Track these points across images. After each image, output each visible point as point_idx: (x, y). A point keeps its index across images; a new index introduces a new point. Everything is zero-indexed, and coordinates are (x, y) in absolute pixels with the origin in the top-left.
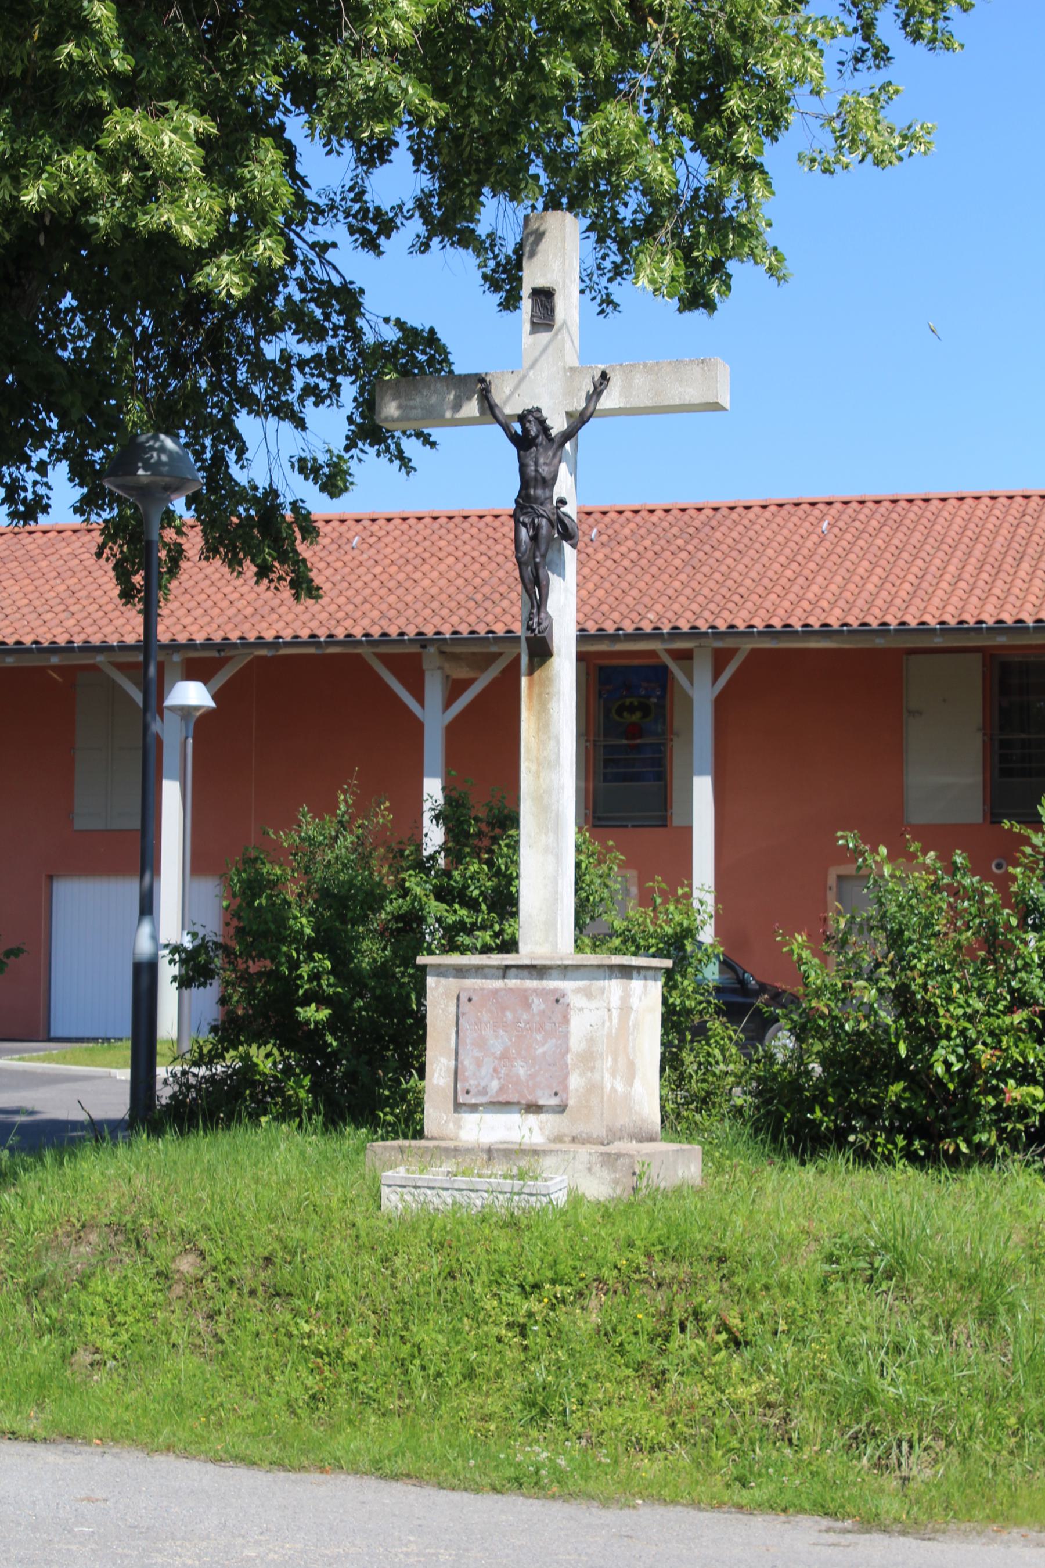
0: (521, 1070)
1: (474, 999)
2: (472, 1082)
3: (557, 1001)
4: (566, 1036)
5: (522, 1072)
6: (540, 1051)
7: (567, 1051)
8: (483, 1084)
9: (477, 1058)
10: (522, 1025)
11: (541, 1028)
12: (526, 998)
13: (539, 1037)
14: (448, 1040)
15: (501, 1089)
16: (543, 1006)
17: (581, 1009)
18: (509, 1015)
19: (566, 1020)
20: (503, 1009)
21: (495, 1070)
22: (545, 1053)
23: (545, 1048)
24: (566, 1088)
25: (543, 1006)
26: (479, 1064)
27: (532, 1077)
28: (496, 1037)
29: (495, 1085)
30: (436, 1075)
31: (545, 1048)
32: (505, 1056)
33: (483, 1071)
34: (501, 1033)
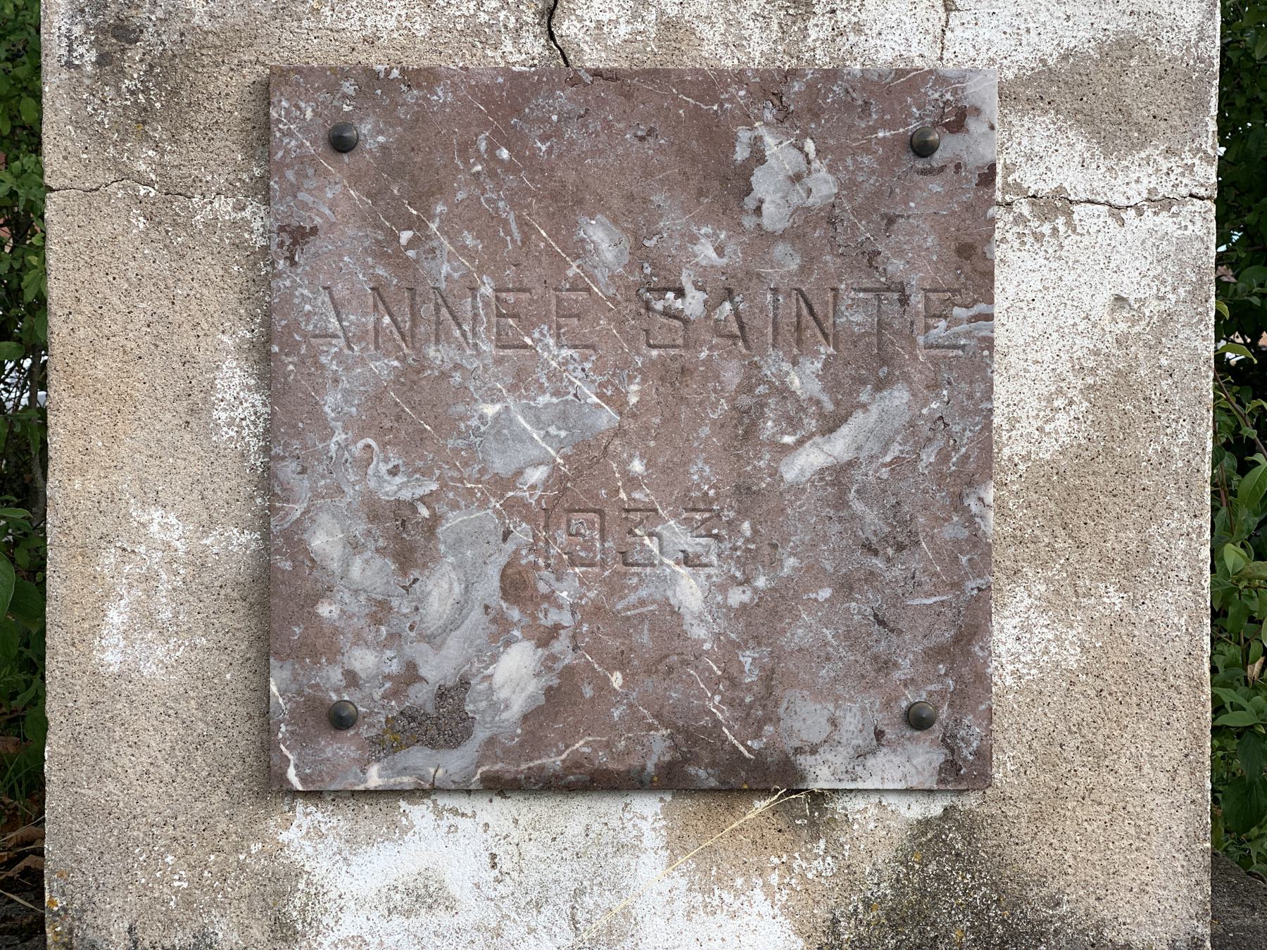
0: (691, 591)
1: (372, 135)
2: (364, 660)
3: (922, 148)
4: (974, 364)
5: (689, 592)
6: (807, 461)
7: (980, 463)
8: (437, 668)
9: (401, 513)
10: (693, 303)
11: (807, 321)
12: (716, 135)
13: (804, 380)
14: (196, 410)
15: (558, 699)
16: (823, 185)
17: (1055, 205)
18: (602, 239)
19: (972, 266)
20: (566, 205)
21: (515, 585)
22: (838, 475)
23: (839, 446)
24: (973, 685)
25: (823, 185)
26: (406, 539)
27: (762, 620)
28: (521, 381)
29: (516, 674)
30: (116, 616)
31: (839, 446)
32: (578, 491)
33: (440, 591)
34: (552, 351)
